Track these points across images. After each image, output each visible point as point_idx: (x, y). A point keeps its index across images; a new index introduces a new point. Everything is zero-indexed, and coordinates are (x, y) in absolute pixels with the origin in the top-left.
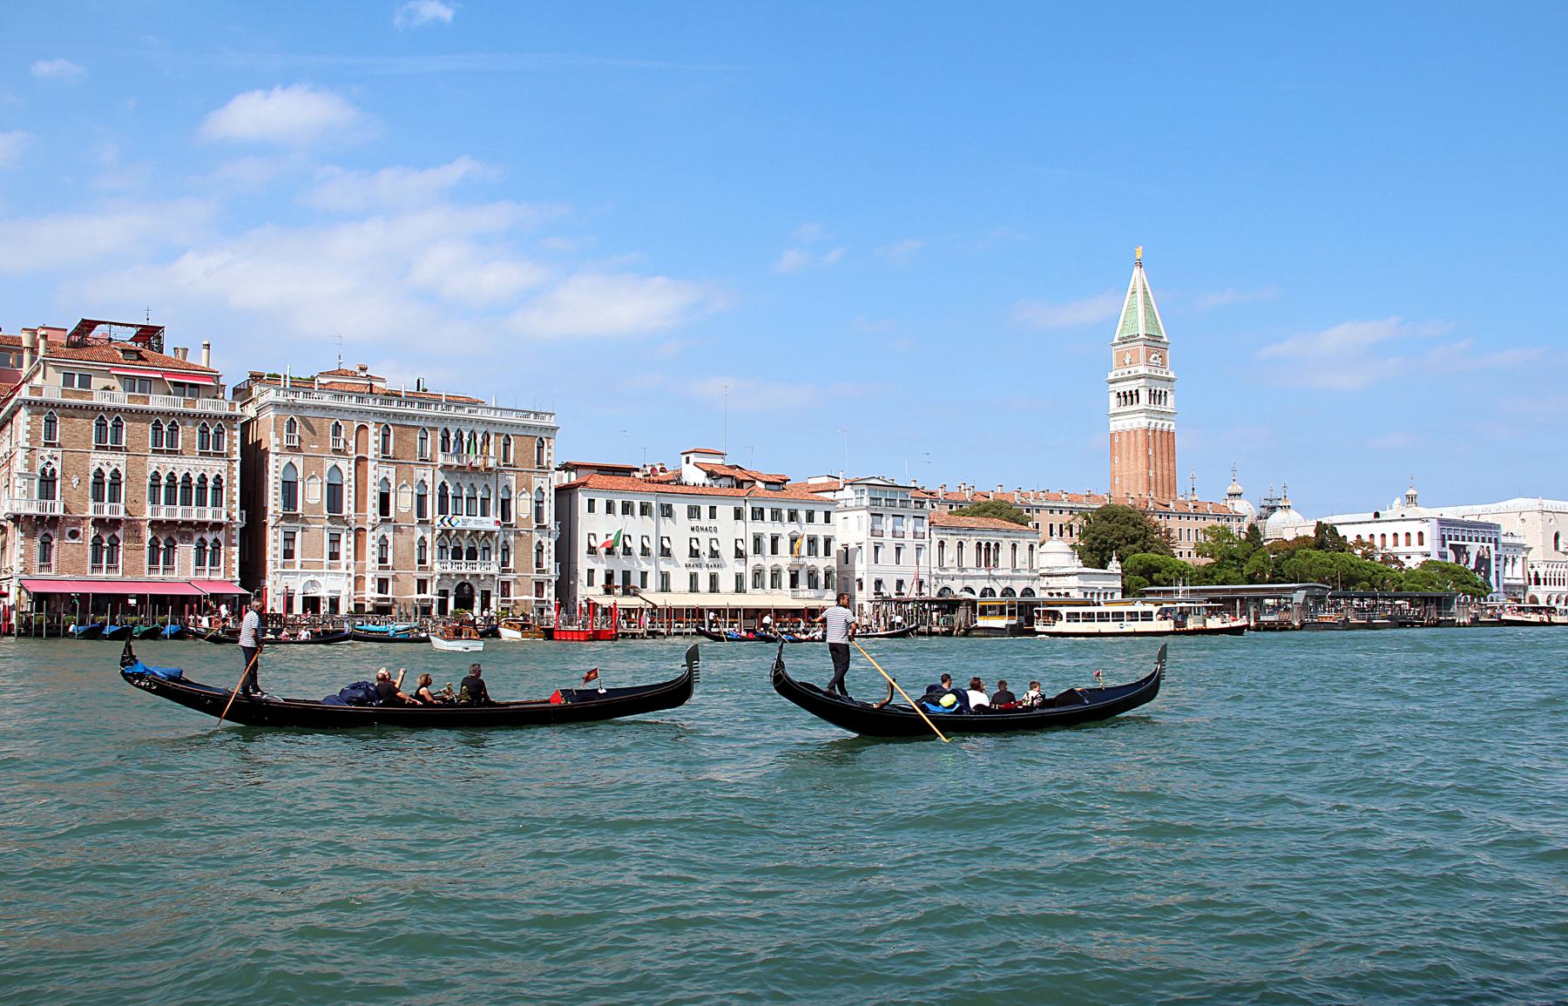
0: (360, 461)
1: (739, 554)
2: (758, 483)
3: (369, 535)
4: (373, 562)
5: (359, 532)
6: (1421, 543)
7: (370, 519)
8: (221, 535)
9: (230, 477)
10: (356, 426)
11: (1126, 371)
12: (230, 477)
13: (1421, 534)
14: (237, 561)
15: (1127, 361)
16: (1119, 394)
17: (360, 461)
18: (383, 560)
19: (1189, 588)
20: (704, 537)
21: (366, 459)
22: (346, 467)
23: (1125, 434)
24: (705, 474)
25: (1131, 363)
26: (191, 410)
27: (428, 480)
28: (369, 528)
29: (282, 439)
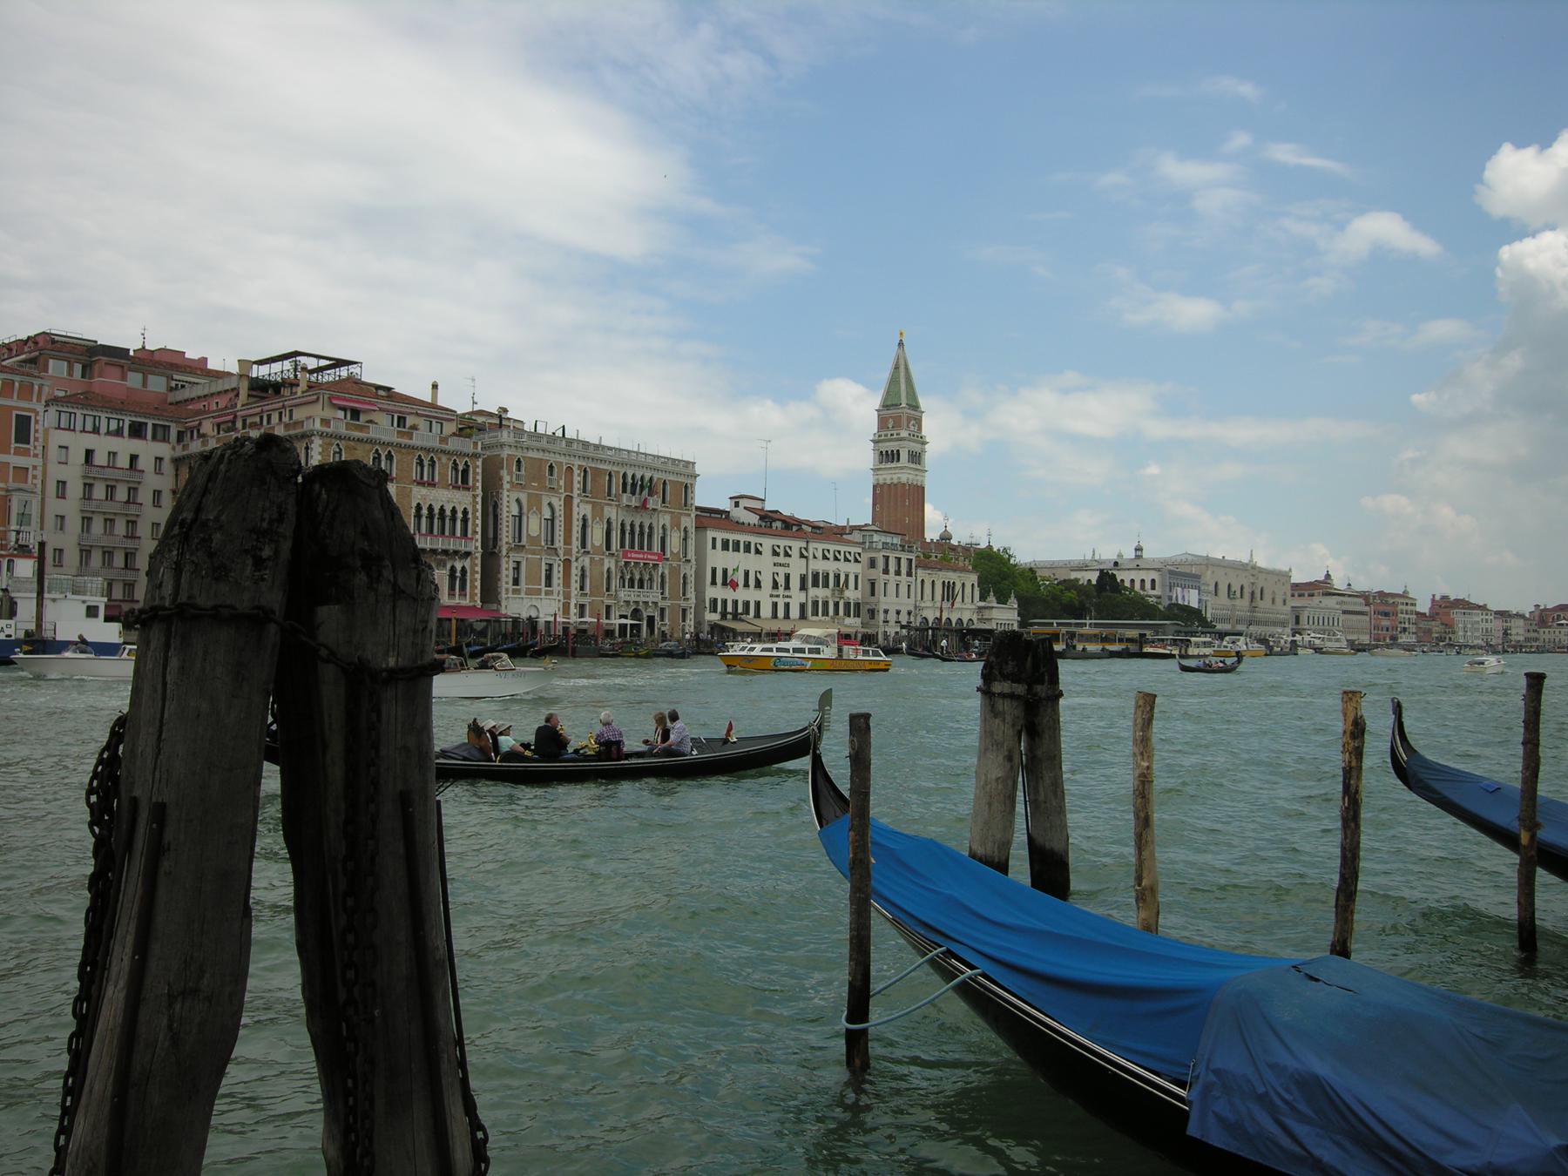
0: (569, 500)
1: (803, 587)
2: (803, 526)
3: (574, 564)
4: (576, 589)
5: (567, 563)
6: (1153, 588)
7: (575, 550)
8: (467, 563)
9: (475, 511)
10: (565, 468)
11: (889, 433)
12: (475, 511)
13: (1153, 581)
14: (479, 587)
15: (890, 426)
16: (881, 452)
17: (569, 500)
18: (582, 588)
19: (1093, 621)
20: (782, 571)
21: (572, 497)
22: (558, 504)
23: (885, 487)
24: (758, 517)
25: (893, 427)
26: (444, 447)
27: (613, 517)
28: (573, 559)
29: (512, 477)
